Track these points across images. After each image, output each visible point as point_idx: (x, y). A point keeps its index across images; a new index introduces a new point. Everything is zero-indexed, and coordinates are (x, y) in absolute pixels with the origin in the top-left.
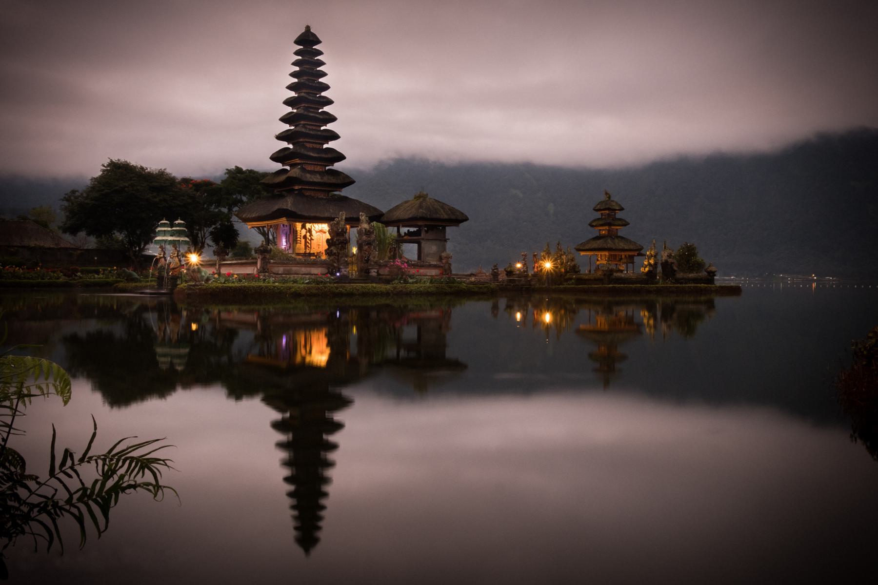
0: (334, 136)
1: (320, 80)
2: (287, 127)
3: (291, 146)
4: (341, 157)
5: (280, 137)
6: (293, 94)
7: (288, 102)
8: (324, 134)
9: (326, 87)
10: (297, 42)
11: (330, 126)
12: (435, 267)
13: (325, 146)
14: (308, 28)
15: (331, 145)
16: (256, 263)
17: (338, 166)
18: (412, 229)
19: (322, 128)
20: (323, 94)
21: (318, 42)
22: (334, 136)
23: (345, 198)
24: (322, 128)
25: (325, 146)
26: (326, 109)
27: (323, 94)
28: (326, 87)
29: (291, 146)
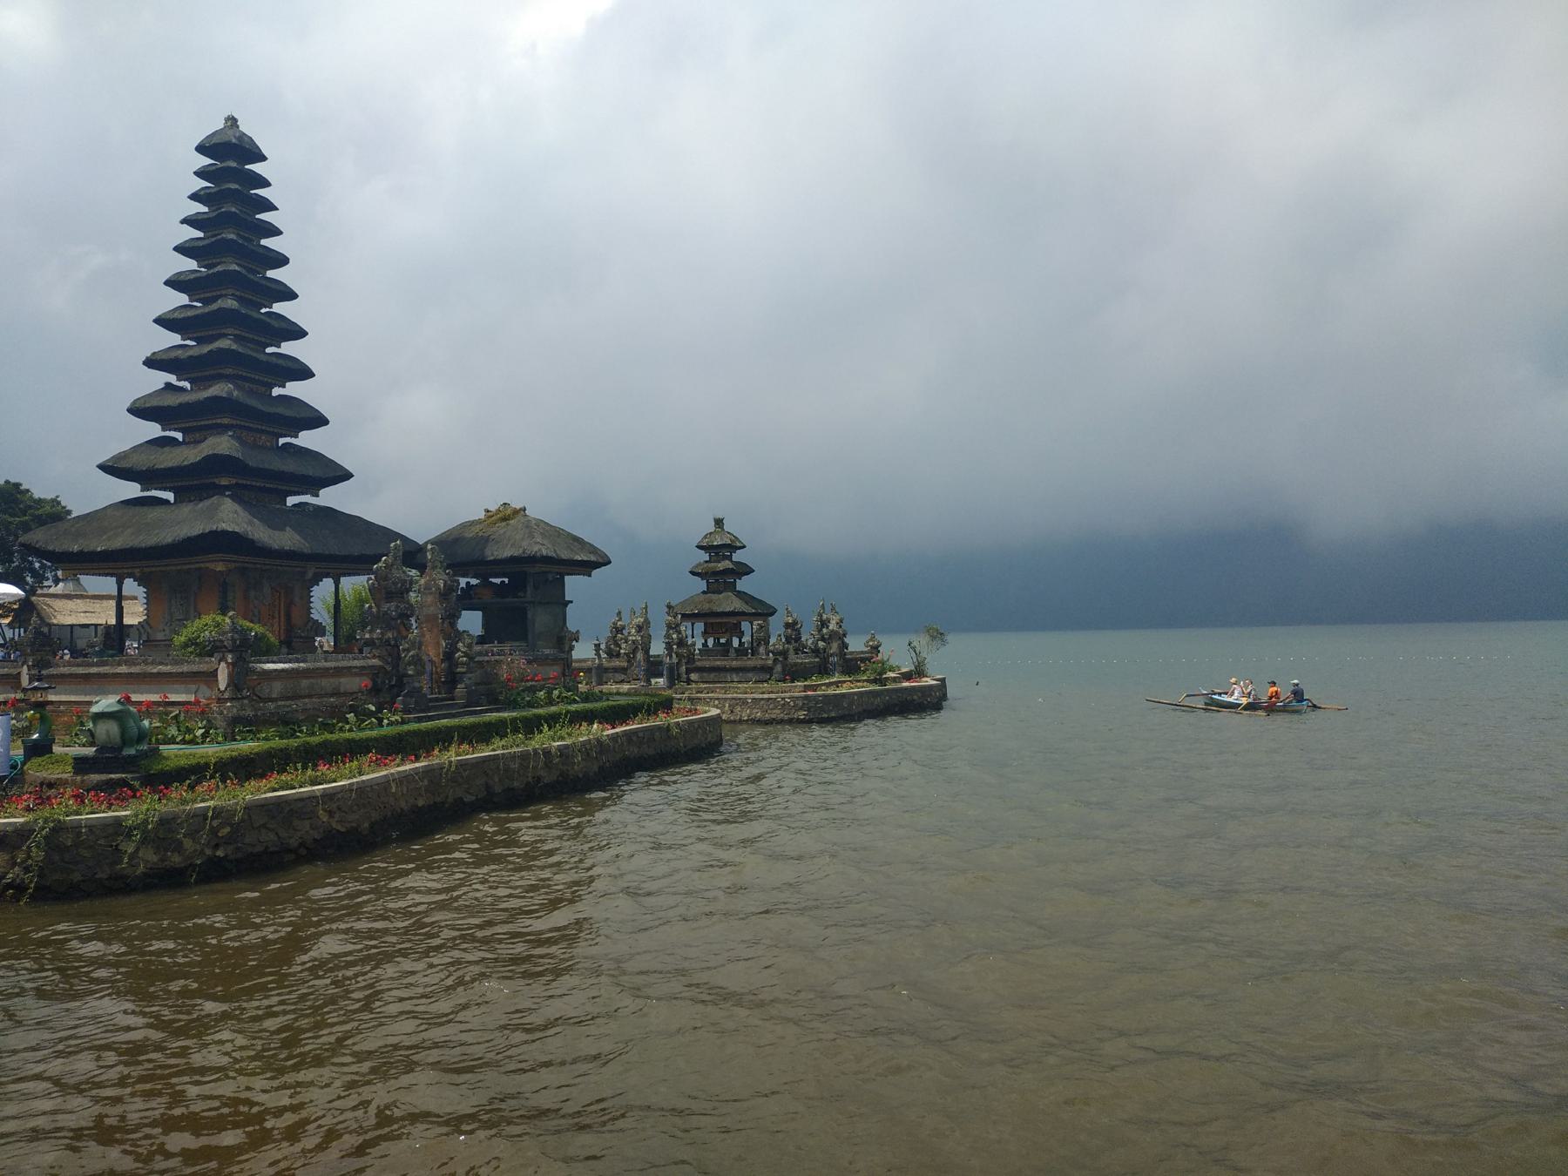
1: (264, 242)
2: (175, 339)
3: (187, 385)
4: (318, 420)
5: (151, 363)
6: (190, 264)
7: (175, 283)
8: (274, 359)
9: (281, 261)
10: (201, 149)
12: (555, 661)
13: (276, 391)
14: (232, 121)
15: (293, 389)
16: (214, 674)
17: (307, 439)
18: (474, 581)
19: (269, 350)
20: (271, 274)
21: (263, 158)
24: (269, 350)
25: (276, 391)
26: (278, 308)
27: (271, 274)
28: (281, 261)
29: (187, 385)
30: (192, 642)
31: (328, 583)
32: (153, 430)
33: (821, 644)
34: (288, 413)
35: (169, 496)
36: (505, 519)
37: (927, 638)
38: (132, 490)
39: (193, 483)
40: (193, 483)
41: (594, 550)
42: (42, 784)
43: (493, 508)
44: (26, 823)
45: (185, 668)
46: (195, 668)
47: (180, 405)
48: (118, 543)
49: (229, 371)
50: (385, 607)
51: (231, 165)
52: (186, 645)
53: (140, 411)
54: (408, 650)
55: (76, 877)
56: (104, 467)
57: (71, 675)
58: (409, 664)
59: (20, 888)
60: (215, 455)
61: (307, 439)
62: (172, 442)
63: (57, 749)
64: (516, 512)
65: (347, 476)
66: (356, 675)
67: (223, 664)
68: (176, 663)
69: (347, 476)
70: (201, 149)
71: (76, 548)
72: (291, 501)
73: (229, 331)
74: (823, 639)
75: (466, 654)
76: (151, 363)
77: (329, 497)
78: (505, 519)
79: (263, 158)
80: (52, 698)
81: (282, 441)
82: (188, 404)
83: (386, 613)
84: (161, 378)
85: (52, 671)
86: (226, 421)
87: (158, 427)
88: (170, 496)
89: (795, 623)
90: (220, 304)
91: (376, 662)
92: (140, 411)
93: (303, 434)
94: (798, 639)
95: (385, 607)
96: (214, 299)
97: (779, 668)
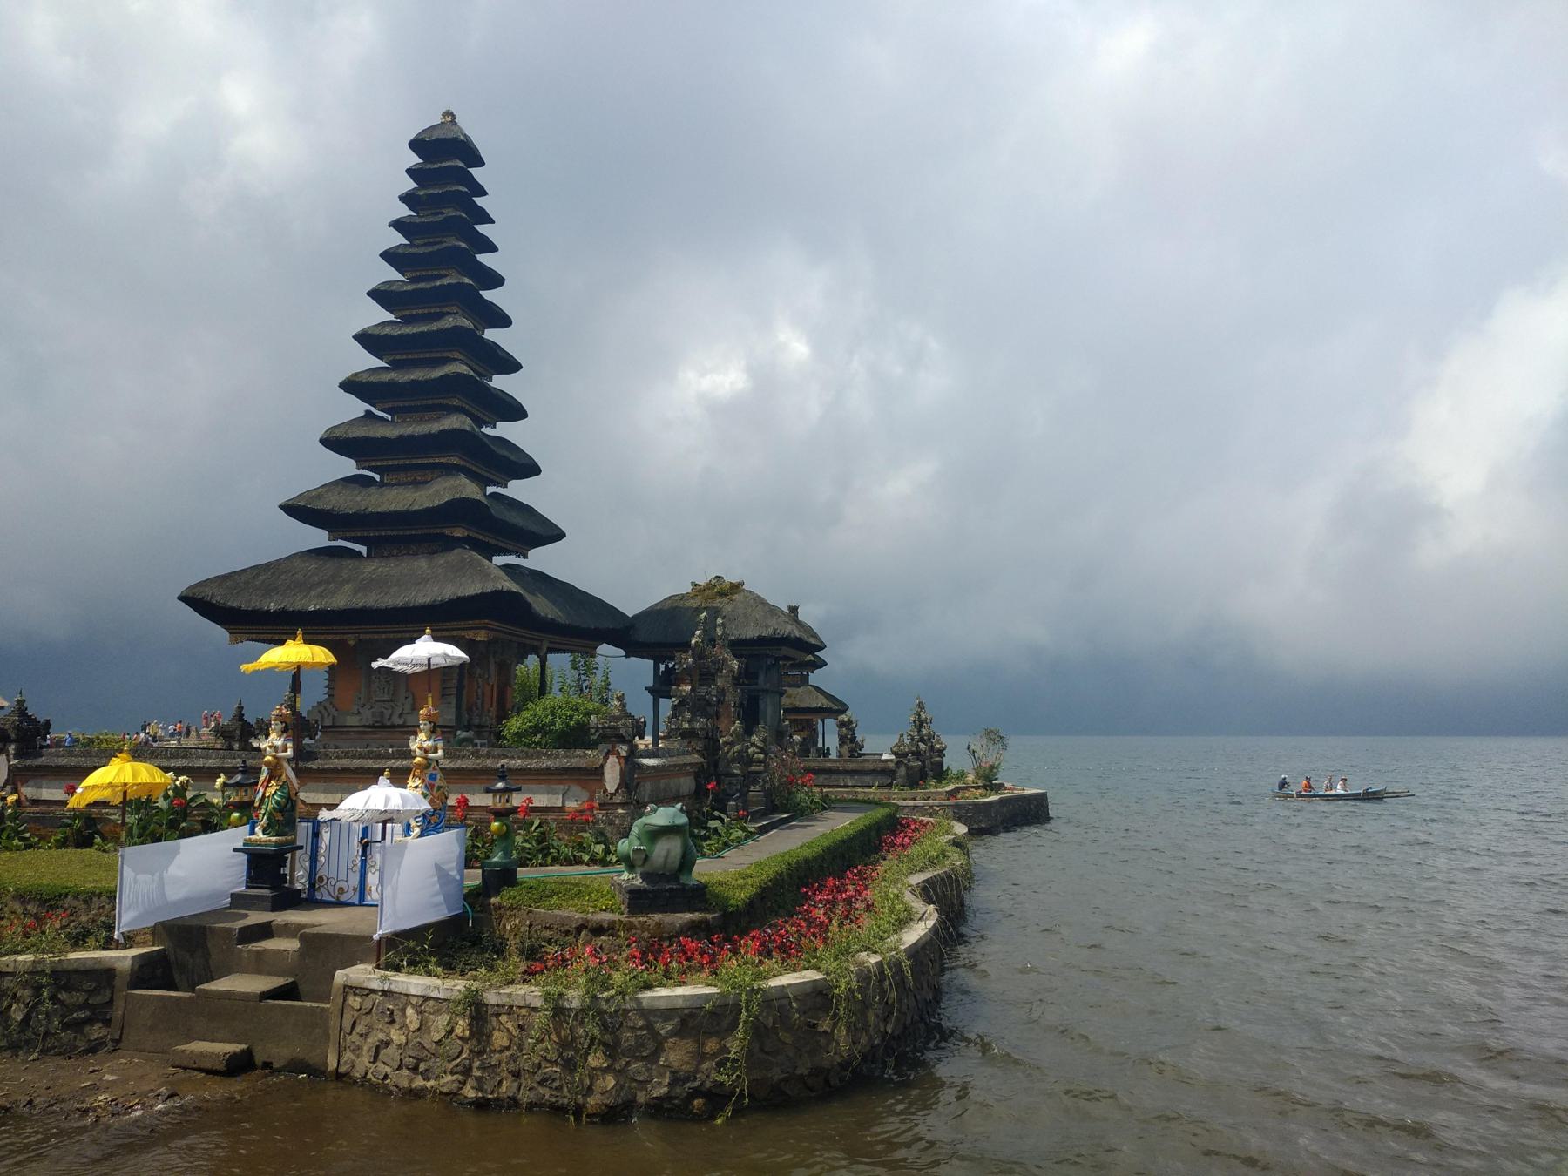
0: (515, 412)
2: (370, 361)
4: (529, 469)
5: (350, 386)
9: (496, 281)
10: (416, 145)
11: (499, 382)
13: (487, 430)
15: (503, 430)
16: (598, 772)
17: (517, 489)
21: (480, 162)
22: (515, 412)
23: (541, 580)
25: (487, 430)
28: (496, 281)
30: (537, 729)
31: (532, 661)
32: (347, 467)
33: (922, 746)
34: (512, 458)
35: (363, 549)
36: (722, 594)
37: (985, 741)
38: (318, 538)
39: (391, 535)
40: (391, 535)
41: (815, 635)
42: (579, 929)
43: (702, 581)
44: (722, 994)
45: (546, 763)
46: (565, 763)
47: (401, 437)
48: (339, 601)
49: (455, 402)
50: (702, 691)
51: (445, 171)
52: (519, 735)
53: (335, 442)
54: (732, 744)
55: (776, 1074)
56: (290, 509)
57: (345, 770)
58: (733, 760)
59: (716, 1098)
60: (464, 500)
61: (517, 489)
62: (368, 482)
63: (523, 873)
64: (736, 587)
65: (553, 534)
66: (688, 774)
67: (612, 759)
68: (527, 756)
69: (556, 535)
70: (416, 145)
71: (273, 607)
72: (499, 560)
73: (456, 355)
74: (922, 740)
75: (762, 751)
76: (350, 386)
77: (540, 559)
78: (722, 594)
79: (480, 162)
80: (517, 800)
81: (490, 490)
82: (412, 437)
83: (703, 698)
84: (356, 407)
85: (314, 765)
86: (455, 461)
87: (352, 463)
88: (363, 549)
89: (850, 722)
90: (448, 323)
91: (696, 758)
92: (335, 442)
93: (513, 484)
94: (853, 739)
95: (702, 691)
96: (439, 316)
97: (902, 771)
